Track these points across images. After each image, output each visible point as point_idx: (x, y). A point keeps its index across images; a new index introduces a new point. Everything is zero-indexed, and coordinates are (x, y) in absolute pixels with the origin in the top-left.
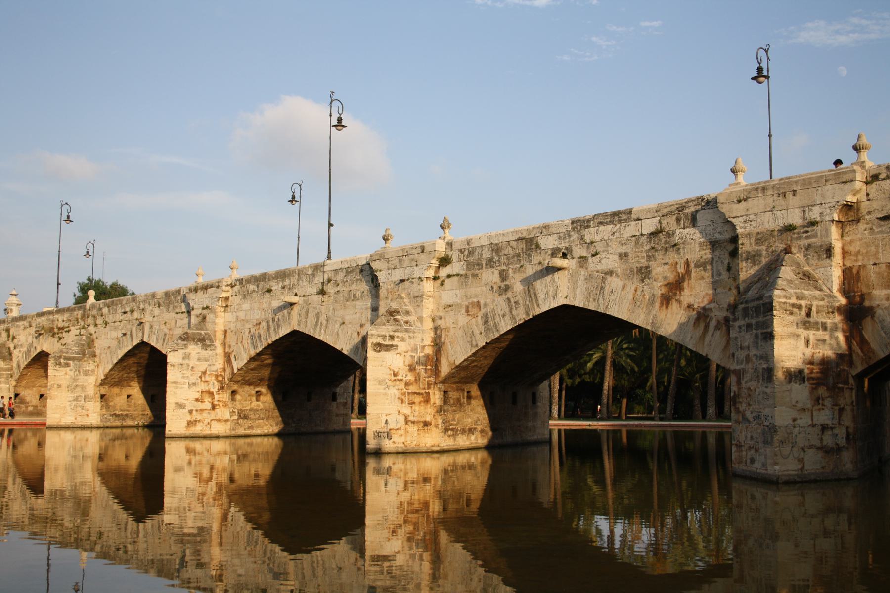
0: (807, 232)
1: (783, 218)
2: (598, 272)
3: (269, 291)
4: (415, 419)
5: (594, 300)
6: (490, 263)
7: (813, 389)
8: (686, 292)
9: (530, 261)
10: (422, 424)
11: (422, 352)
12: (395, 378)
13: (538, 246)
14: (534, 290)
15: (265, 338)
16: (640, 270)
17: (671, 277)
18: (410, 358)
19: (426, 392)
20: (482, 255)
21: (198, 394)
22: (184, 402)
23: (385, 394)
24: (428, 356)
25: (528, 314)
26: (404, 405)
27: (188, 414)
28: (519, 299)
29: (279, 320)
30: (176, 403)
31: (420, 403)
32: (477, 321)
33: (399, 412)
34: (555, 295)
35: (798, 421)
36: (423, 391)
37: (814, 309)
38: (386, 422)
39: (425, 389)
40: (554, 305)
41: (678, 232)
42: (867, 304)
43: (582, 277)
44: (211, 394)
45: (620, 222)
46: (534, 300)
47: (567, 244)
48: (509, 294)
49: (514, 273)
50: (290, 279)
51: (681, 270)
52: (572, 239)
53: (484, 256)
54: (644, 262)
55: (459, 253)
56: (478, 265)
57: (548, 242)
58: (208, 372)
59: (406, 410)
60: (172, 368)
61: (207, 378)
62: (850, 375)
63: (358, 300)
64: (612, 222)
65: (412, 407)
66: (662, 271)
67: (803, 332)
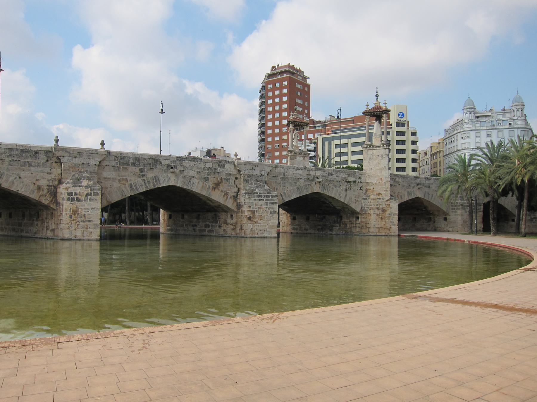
0: (261, 177)
6: (133, 164)
8: (221, 187)
9: (156, 167)
13: (161, 163)
16: (205, 178)
17: (216, 182)
20: (129, 161)
25: (154, 186)
34: (168, 181)
41: (218, 169)
45: (198, 161)
46: (158, 182)
47: (174, 165)
48: (145, 178)
51: (219, 180)
53: (130, 161)
54: (206, 176)
55: (115, 157)
56: (127, 164)
63: (34, 167)
64: (194, 161)
66: (213, 180)
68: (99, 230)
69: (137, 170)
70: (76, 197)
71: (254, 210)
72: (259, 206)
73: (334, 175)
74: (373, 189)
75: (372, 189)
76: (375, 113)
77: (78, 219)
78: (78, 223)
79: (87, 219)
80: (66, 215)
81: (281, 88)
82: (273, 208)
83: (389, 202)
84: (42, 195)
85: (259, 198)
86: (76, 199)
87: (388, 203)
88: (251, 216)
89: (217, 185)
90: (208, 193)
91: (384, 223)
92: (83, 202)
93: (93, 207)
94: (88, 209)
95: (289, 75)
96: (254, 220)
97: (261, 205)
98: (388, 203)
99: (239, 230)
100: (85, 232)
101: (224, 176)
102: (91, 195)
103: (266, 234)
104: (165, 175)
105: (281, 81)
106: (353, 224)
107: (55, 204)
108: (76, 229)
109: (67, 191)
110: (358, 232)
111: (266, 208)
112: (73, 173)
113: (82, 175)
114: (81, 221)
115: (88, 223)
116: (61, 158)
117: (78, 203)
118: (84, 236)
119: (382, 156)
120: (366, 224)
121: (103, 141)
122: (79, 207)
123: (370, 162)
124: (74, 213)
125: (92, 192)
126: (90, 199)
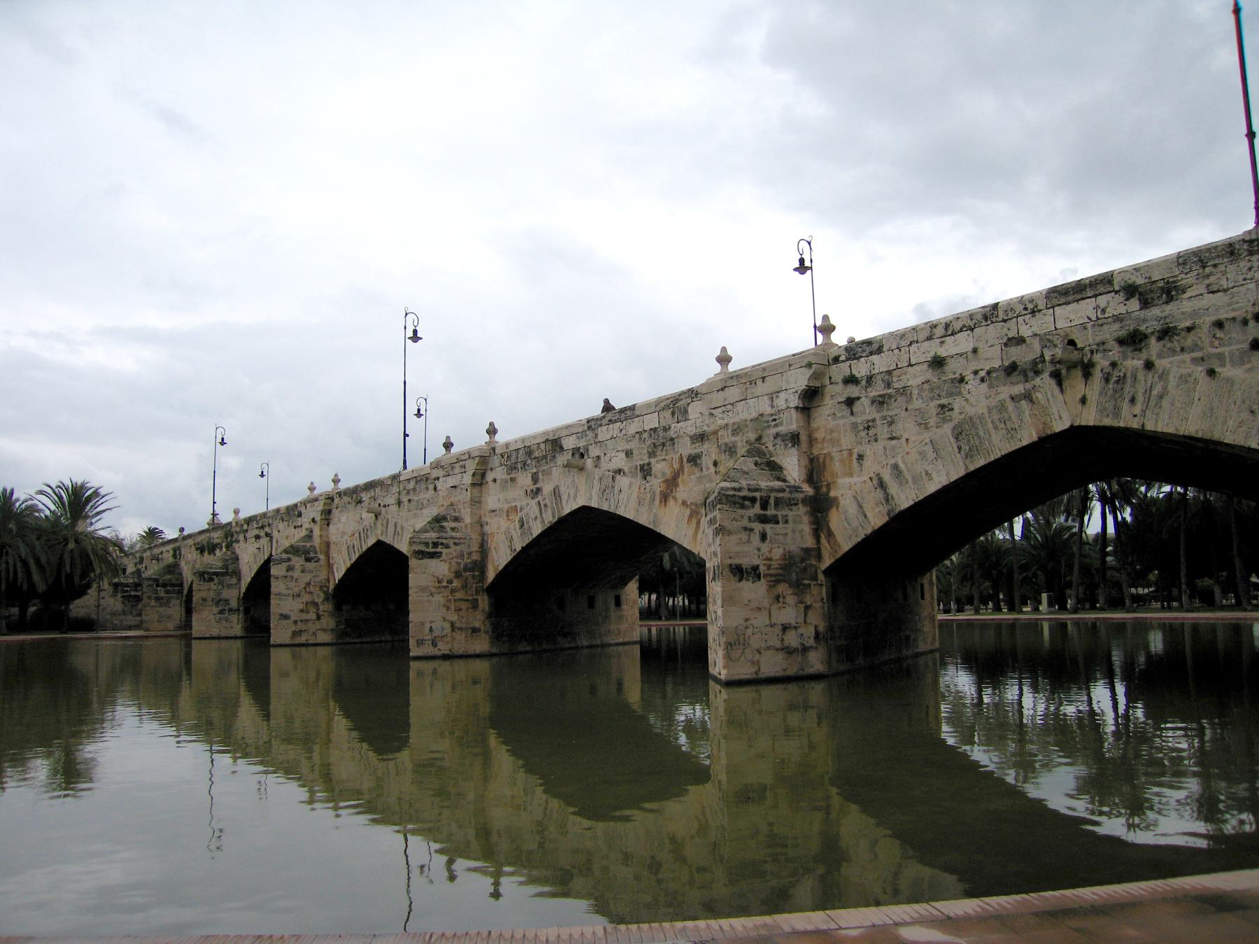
0: (775, 420)
1: (755, 407)
2: (609, 471)
3: (360, 502)
4: (463, 626)
5: (606, 499)
7: (771, 586)
8: (681, 488)
10: (470, 631)
11: (468, 558)
12: (440, 585)
13: (561, 448)
14: (559, 491)
16: (642, 467)
18: (455, 564)
19: (473, 599)
21: (302, 605)
22: (289, 613)
23: (429, 601)
24: (475, 563)
26: (450, 612)
27: (293, 625)
28: (547, 501)
29: (367, 530)
30: (281, 615)
31: (468, 609)
32: (515, 526)
33: (444, 619)
35: (753, 621)
36: (471, 598)
37: (772, 501)
38: (431, 629)
39: (472, 595)
40: (575, 507)
41: (673, 426)
42: (832, 494)
43: (597, 478)
44: (316, 604)
48: (540, 498)
50: (375, 491)
51: (676, 466)
52: (588, 438)
53: (519, 460)
57: (569, 443)
58: (312, 583)
59: (454, 618)
60: (276, 580)
61: (312, 589)
62: (819, 571)
65: (458, 614)
67: (758, 527)
69: (529, 481)
73: (1189, 293)
90: (652, 516)
121: (491, 424)
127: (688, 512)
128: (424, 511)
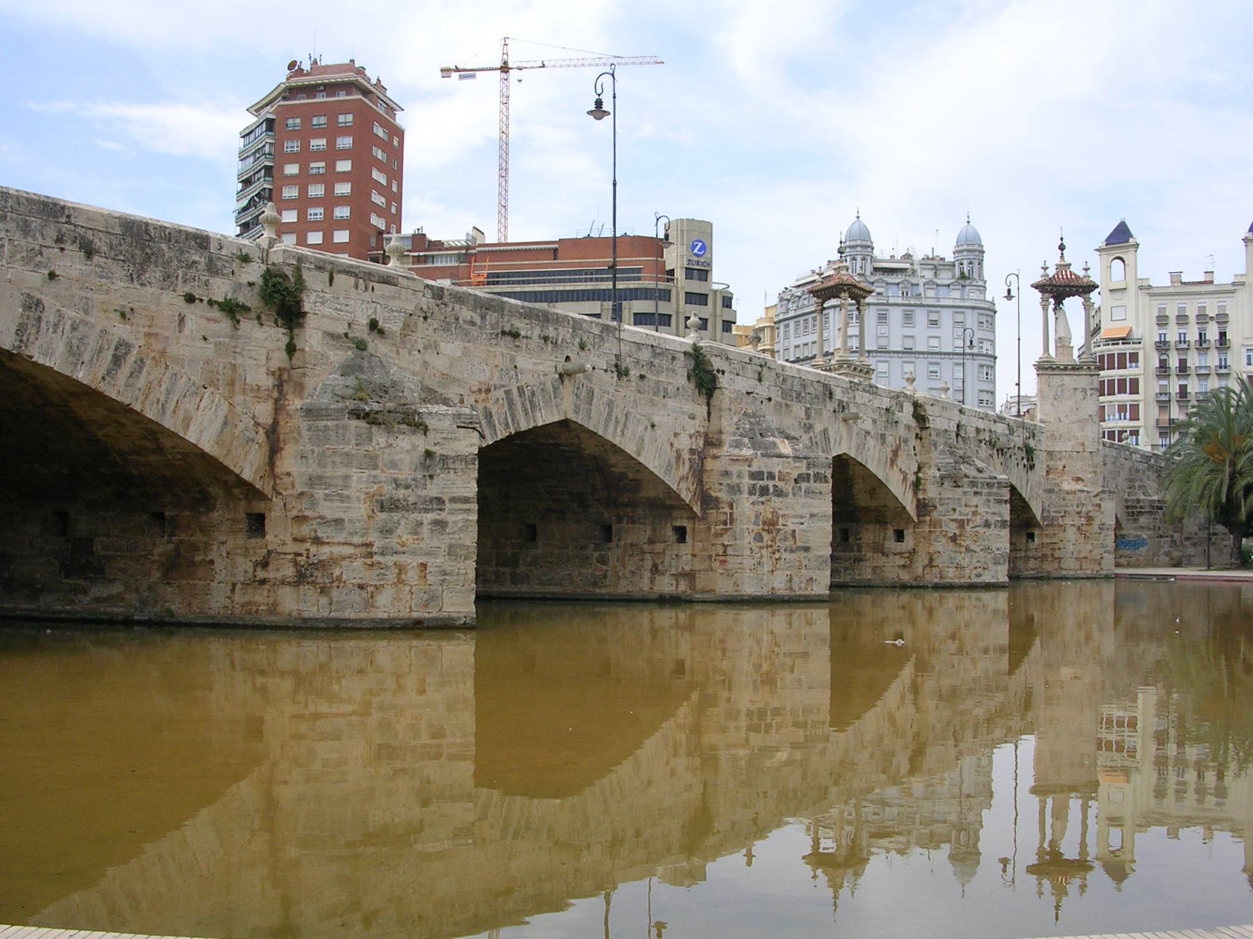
9: (825, 406)
15: (502, 421)
16: (881, 434)
28: (818, 440)
29: (533, 394)
40: (840, 453)
48: (811, 434)
49: (815, 414)
63: (670, 397)
68: (828, 573)
70: (771, 484)
71: (962, 518)
72: (973, 509)
74: (1064, 467)
75: (1061, 468)
76: (1068, 289)
77: (778, 544)
78: (777, 556)
79: (801, 544)
80: (746, 534)
81: (332, 132)
82: (1000, 515)
83: (1098, 498)
84: (682, 478)
85: (972, 488)
86: (771, 491)
87: (1097, 501)
88: (957, 532)
89: (895, 453)
91: (1089, 547)
92: (790, 499)
93: (815, 512)
94: (802, 517)
95: (360, 97)
96: (963, 543)
97: (977, 506)
98: (1097, 501)
99: (924, 567)
100: (795, 579)
101: (902, 431)
102: (808, 481)
103: (987, 578)
104: (836, 426)
105: (332, 111)
106: (1020, 550)
107: (699, 504)
108: (773, 571)
109: (748, 468)
110: (1033, 570)
111: (987, 512)
112: (735, 419)
113: (758, 423)
114: (785, 550)
115: (802, 554)
116: (720, 375)
117: (777, 502)
118: (791, 589)
119: (1084, 390)
120: (1053, 549)
122: (781, 512)
123: (1055, 403)
124: (766, 528)
125: (811, 472)
126: (808, 492)
127: (902, 477)
128: (670, 403)
